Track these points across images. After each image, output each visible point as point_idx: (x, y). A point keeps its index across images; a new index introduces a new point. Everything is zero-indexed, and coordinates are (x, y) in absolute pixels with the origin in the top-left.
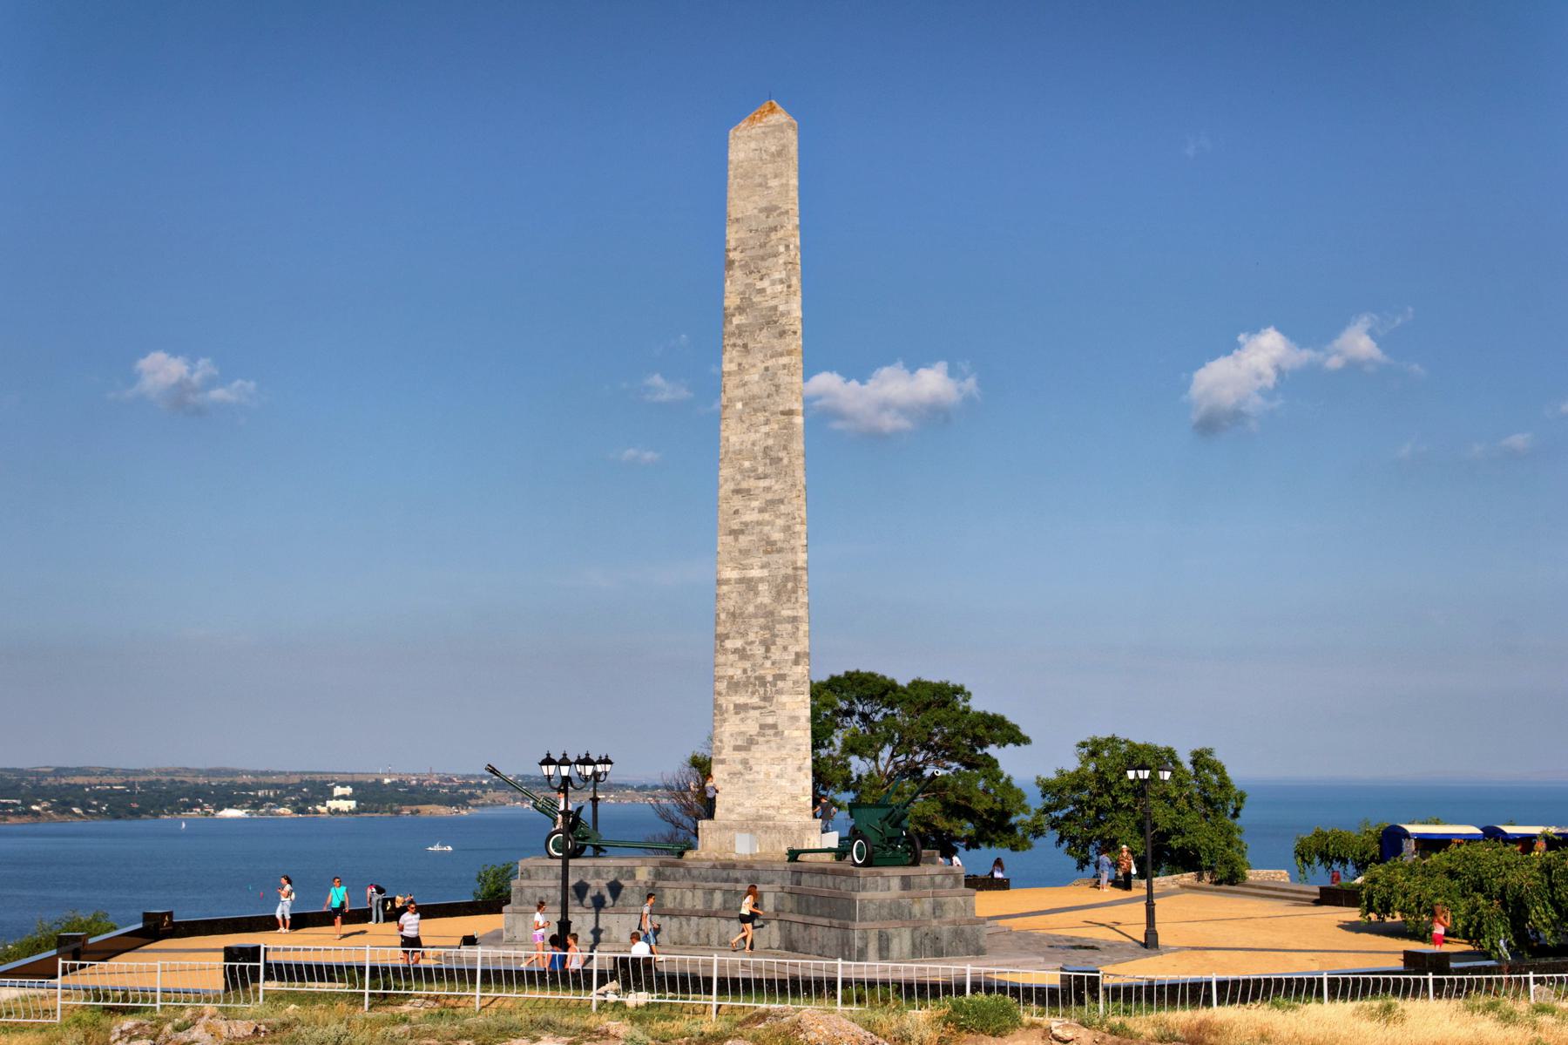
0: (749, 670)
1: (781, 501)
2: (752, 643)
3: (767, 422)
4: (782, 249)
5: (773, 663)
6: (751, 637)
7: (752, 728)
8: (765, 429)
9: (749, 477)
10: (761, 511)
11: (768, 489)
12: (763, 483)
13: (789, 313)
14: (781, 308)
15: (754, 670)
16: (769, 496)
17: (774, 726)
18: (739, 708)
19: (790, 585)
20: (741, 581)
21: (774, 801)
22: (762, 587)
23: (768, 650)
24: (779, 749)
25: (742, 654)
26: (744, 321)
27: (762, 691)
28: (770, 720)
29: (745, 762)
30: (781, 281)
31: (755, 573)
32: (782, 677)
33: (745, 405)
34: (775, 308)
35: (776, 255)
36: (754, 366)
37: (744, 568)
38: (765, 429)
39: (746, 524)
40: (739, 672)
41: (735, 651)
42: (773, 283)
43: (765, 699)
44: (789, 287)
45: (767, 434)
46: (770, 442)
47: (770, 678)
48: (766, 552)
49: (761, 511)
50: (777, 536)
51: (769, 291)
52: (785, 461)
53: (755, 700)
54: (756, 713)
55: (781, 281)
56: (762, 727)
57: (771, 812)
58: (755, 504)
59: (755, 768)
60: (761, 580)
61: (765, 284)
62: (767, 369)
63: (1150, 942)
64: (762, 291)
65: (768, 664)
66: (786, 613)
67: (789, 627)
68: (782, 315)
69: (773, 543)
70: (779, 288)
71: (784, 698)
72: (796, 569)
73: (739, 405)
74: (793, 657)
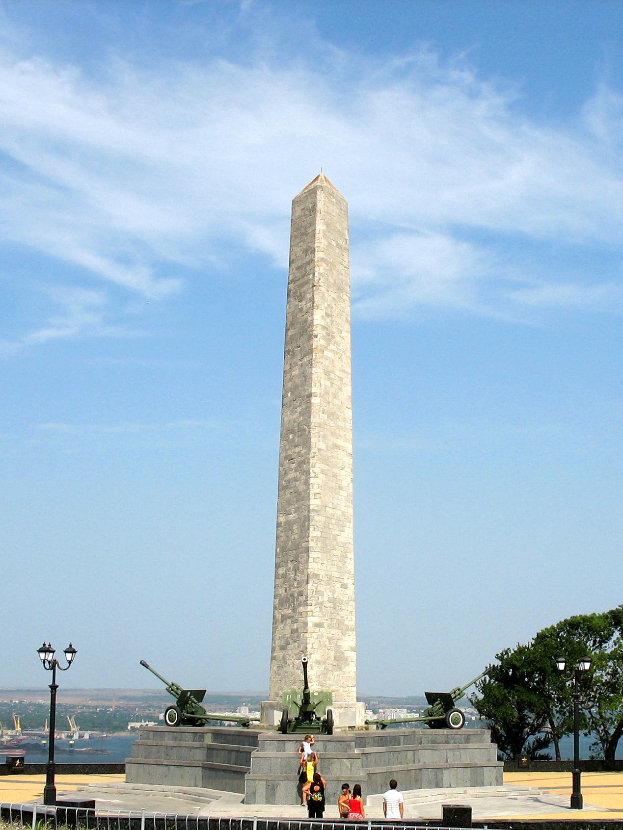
0: (288, 589)
2: (290, 568)
7: (288, 632)
9: (292, 446)
12: (297, 450)
15: (290, 590)
16: (300, 459)
17: (297, 631)
18: (284, 618)
19: (307, 524)
22: (295, 527)
25: (284, 576)
26: (293, 333)
28: (295, 626)
29: (284, 658)
34: (306, 321)
36: (296, 364)
38: (299, 410)
39: (289, 481)
43: (294, 610)
50: (302, 488)
56: (293, 631)
58: (293, 466)
59: (288, 662)
60: (295, 522)
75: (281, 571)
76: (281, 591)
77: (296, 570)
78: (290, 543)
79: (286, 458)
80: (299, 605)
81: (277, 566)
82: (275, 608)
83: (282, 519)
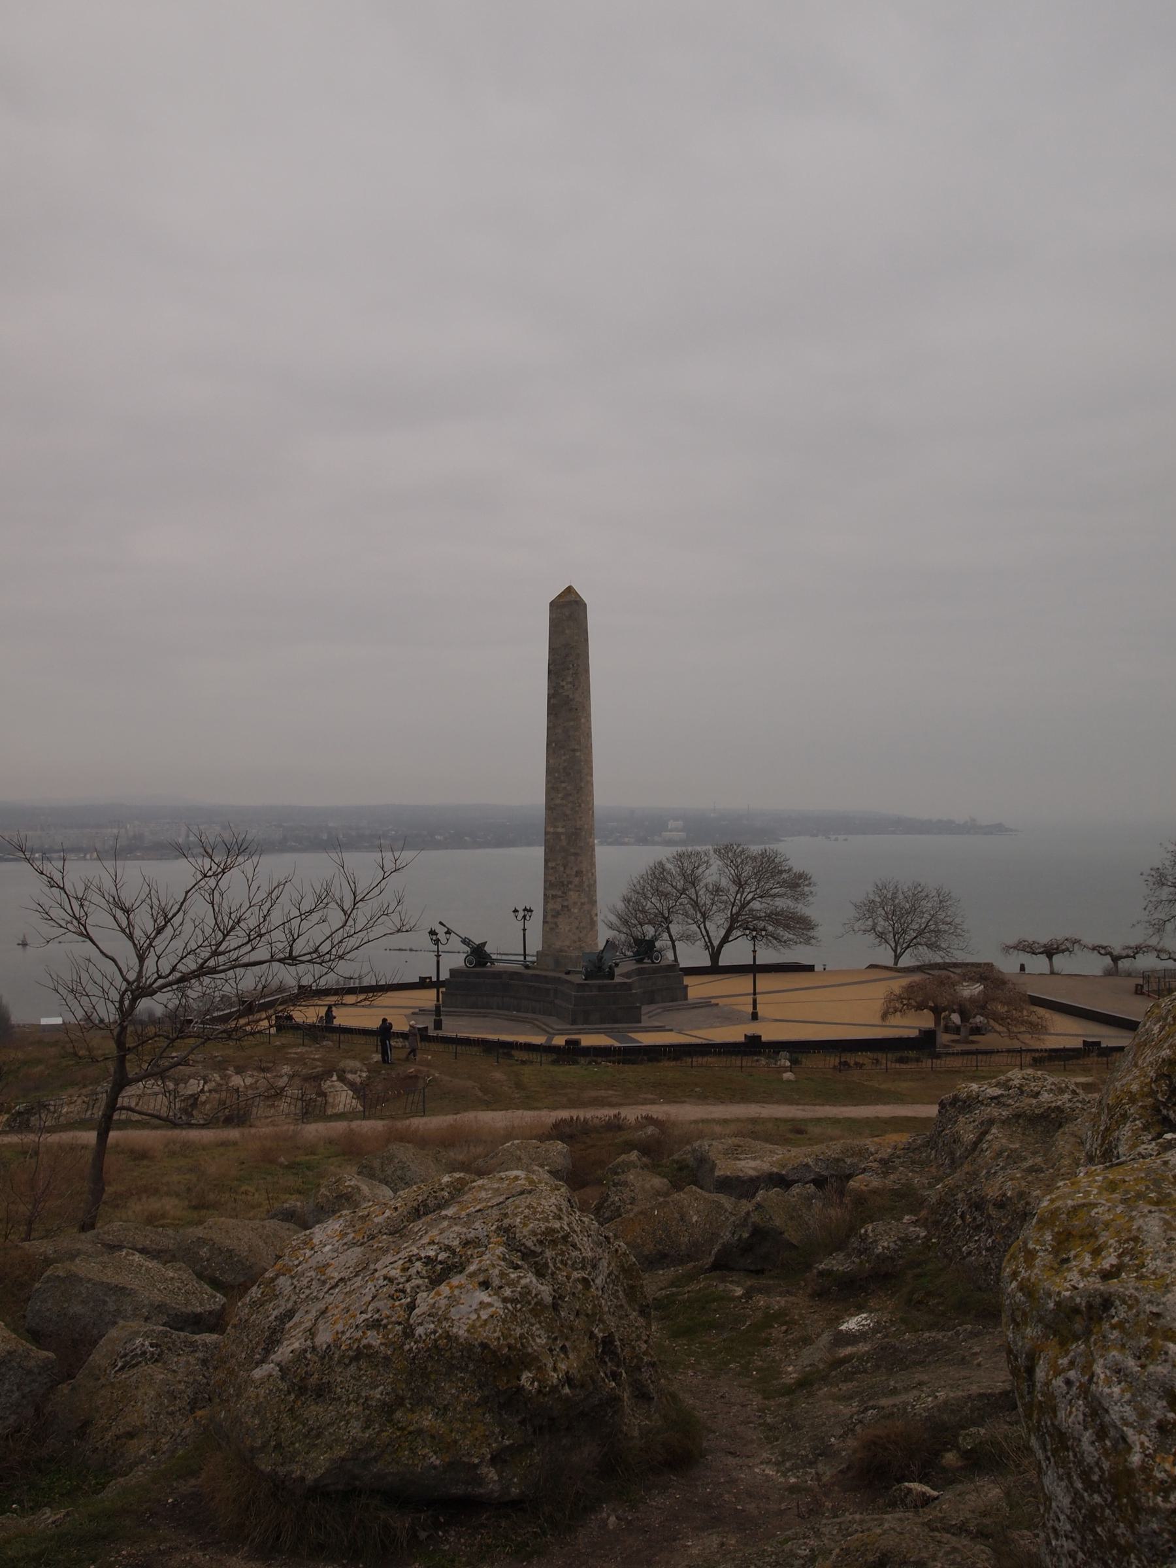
1: (570, 795)
3: (564, 754)
4: (571, 666)
5: (567, 876)
6: (559, 862)
7: (559, 908)
8: (564, 758)
10: (562, 799)
11: (565, 788)
12: (563, 785)
13: (574, 699)
14: (571, 697)
17: (567, 907)
18: (554, 897)
20: (553, 833)
21: (567, 943)
22: (563, 837)
23: (565, 869)
24: (569, 917)
27: (562, 888)
28: (565, 904)
29: (556, 924)
30: (570, 683)
31: (560, 830)
32: (571, 883)
33: (556, 745)
35: (568, 669)
37: (556, 827)
38: (564, 758)
40: (554, 878)
41: (552, 868)
42: (567, 683)
43: (564, 893)
44: (574, 686)
45: (565, 761)
46: (566, 764)
47: (565, 883)
48: (564, 820)
49: (562, 799)
50: (568, 812)
51: (565, 687)
52: (572, 774)
53: (559, 893)
54: (559, 900)
55: (570, 683)
57: (566, 949)
58: (560, 795)
59: (560, 927)
60: (562, 833)
61: (564, 683)
62: (565, 727)
63: (755, 1016)
64: (563, 686)
65: (565, 875)
66: (572, 850)
67: (573, 857)
68: (571, 700)
69: (566, 815)
70: (570, 686)
71: (572, 893)
72: (576, 829)
73: (554, 745)
74: (574, 873)
75: (550, 864)
76: (552, 879)
77: (565, 866)
78: (558, 848)
79: (553, 788)
80: (570, 890)
81: (546, 861)
82: (545, 888)
83: (552, 830)
